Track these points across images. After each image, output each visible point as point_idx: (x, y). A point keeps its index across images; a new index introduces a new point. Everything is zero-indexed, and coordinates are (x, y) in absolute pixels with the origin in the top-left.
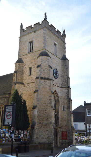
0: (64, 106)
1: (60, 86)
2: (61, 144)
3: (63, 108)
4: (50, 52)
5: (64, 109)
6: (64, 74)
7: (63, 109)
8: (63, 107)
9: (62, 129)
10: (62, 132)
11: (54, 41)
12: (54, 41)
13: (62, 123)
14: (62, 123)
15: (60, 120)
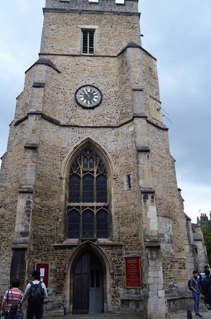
0: (129, 176)
1: (111, 124)
2: (123, 301)
3: (126, 183)
4: (64, 53)
5: (130, 187)
6: (123, 87)
7: (126, 187)
8: (125, 179)
9: (126, 249)
10: (127, 259)
11: (79, 26)
12: (79, 26)
13: (123, 229)
14: (123, 229)
15: (115, 224)
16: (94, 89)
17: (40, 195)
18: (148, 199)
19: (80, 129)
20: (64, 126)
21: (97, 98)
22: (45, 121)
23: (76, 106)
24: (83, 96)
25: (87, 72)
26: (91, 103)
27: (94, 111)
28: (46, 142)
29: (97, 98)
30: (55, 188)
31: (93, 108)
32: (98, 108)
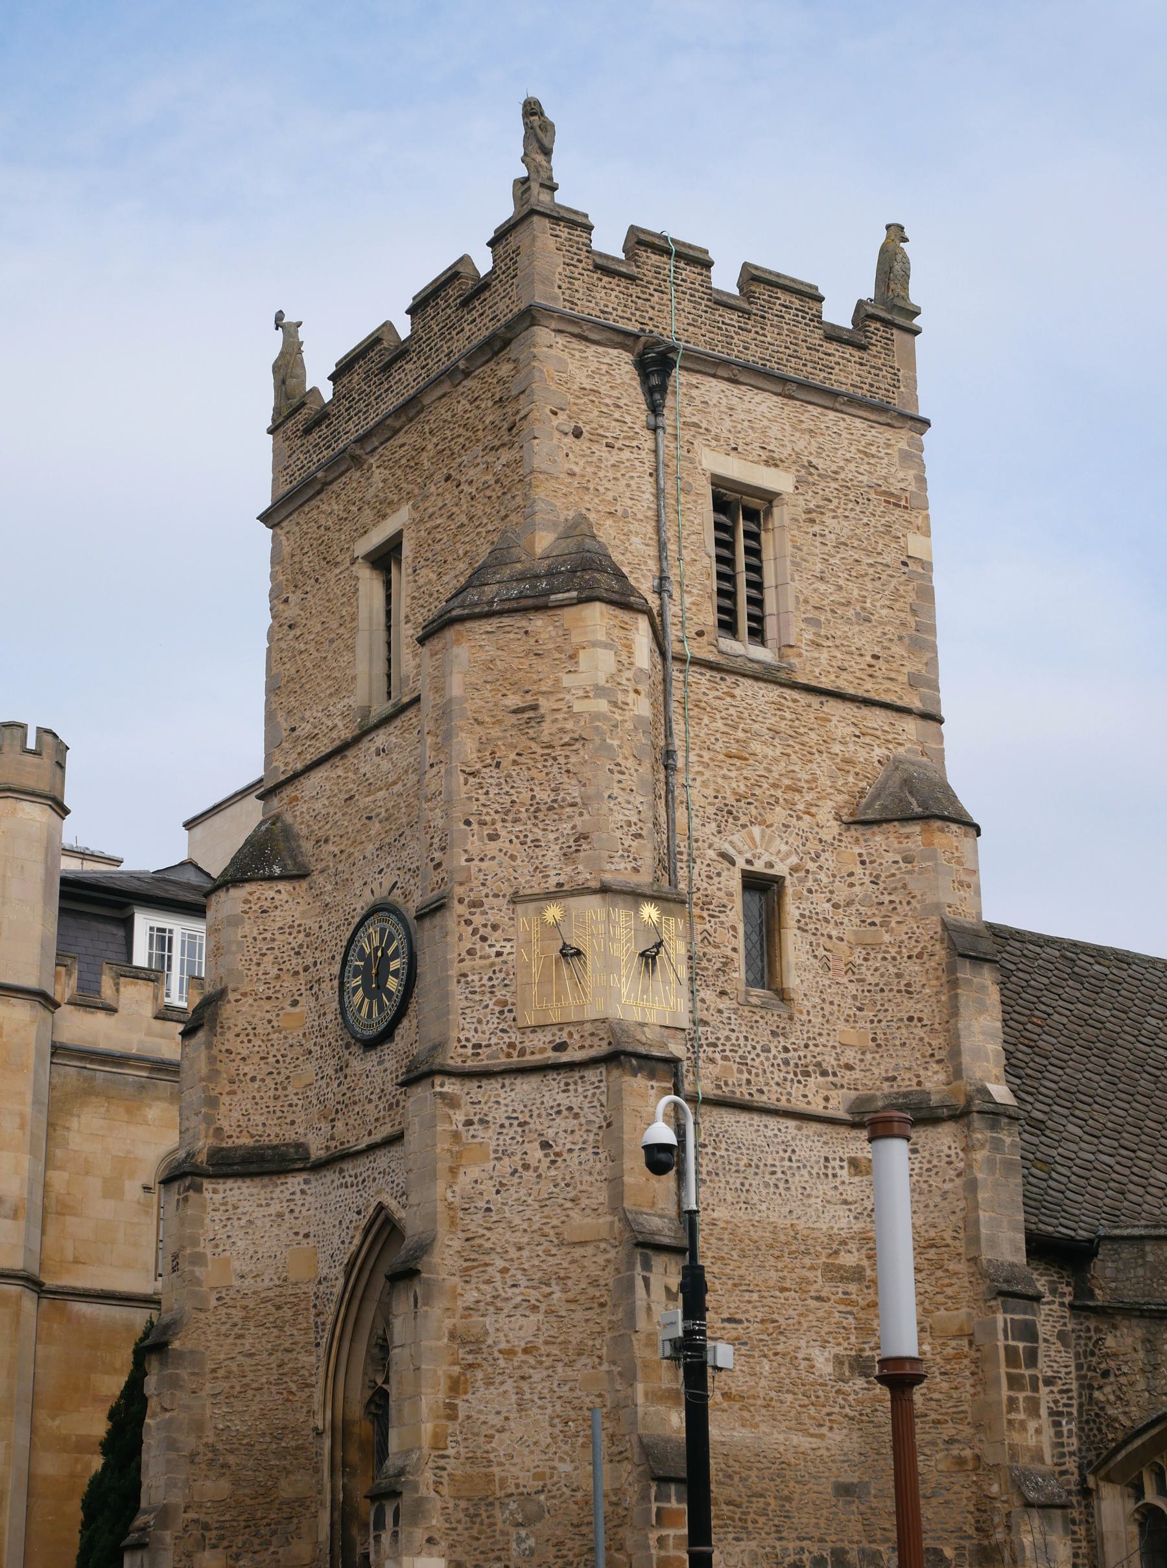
16: (391, 925)
17: (222, 1538)
18: (384, 1527)
19: (360, 1167)
20: (319, 1166)
21: (396, 974)
22: (230, 1183)
23: (348, 1046)
24: (358, 981)
25: (376, 827)
26: (381, 1009)
27: (393, 1046)
28: (236, 1283)
29: (396, 974)
30: (286, 1490)
31: (386, 1036)
32: (405, 1022)
